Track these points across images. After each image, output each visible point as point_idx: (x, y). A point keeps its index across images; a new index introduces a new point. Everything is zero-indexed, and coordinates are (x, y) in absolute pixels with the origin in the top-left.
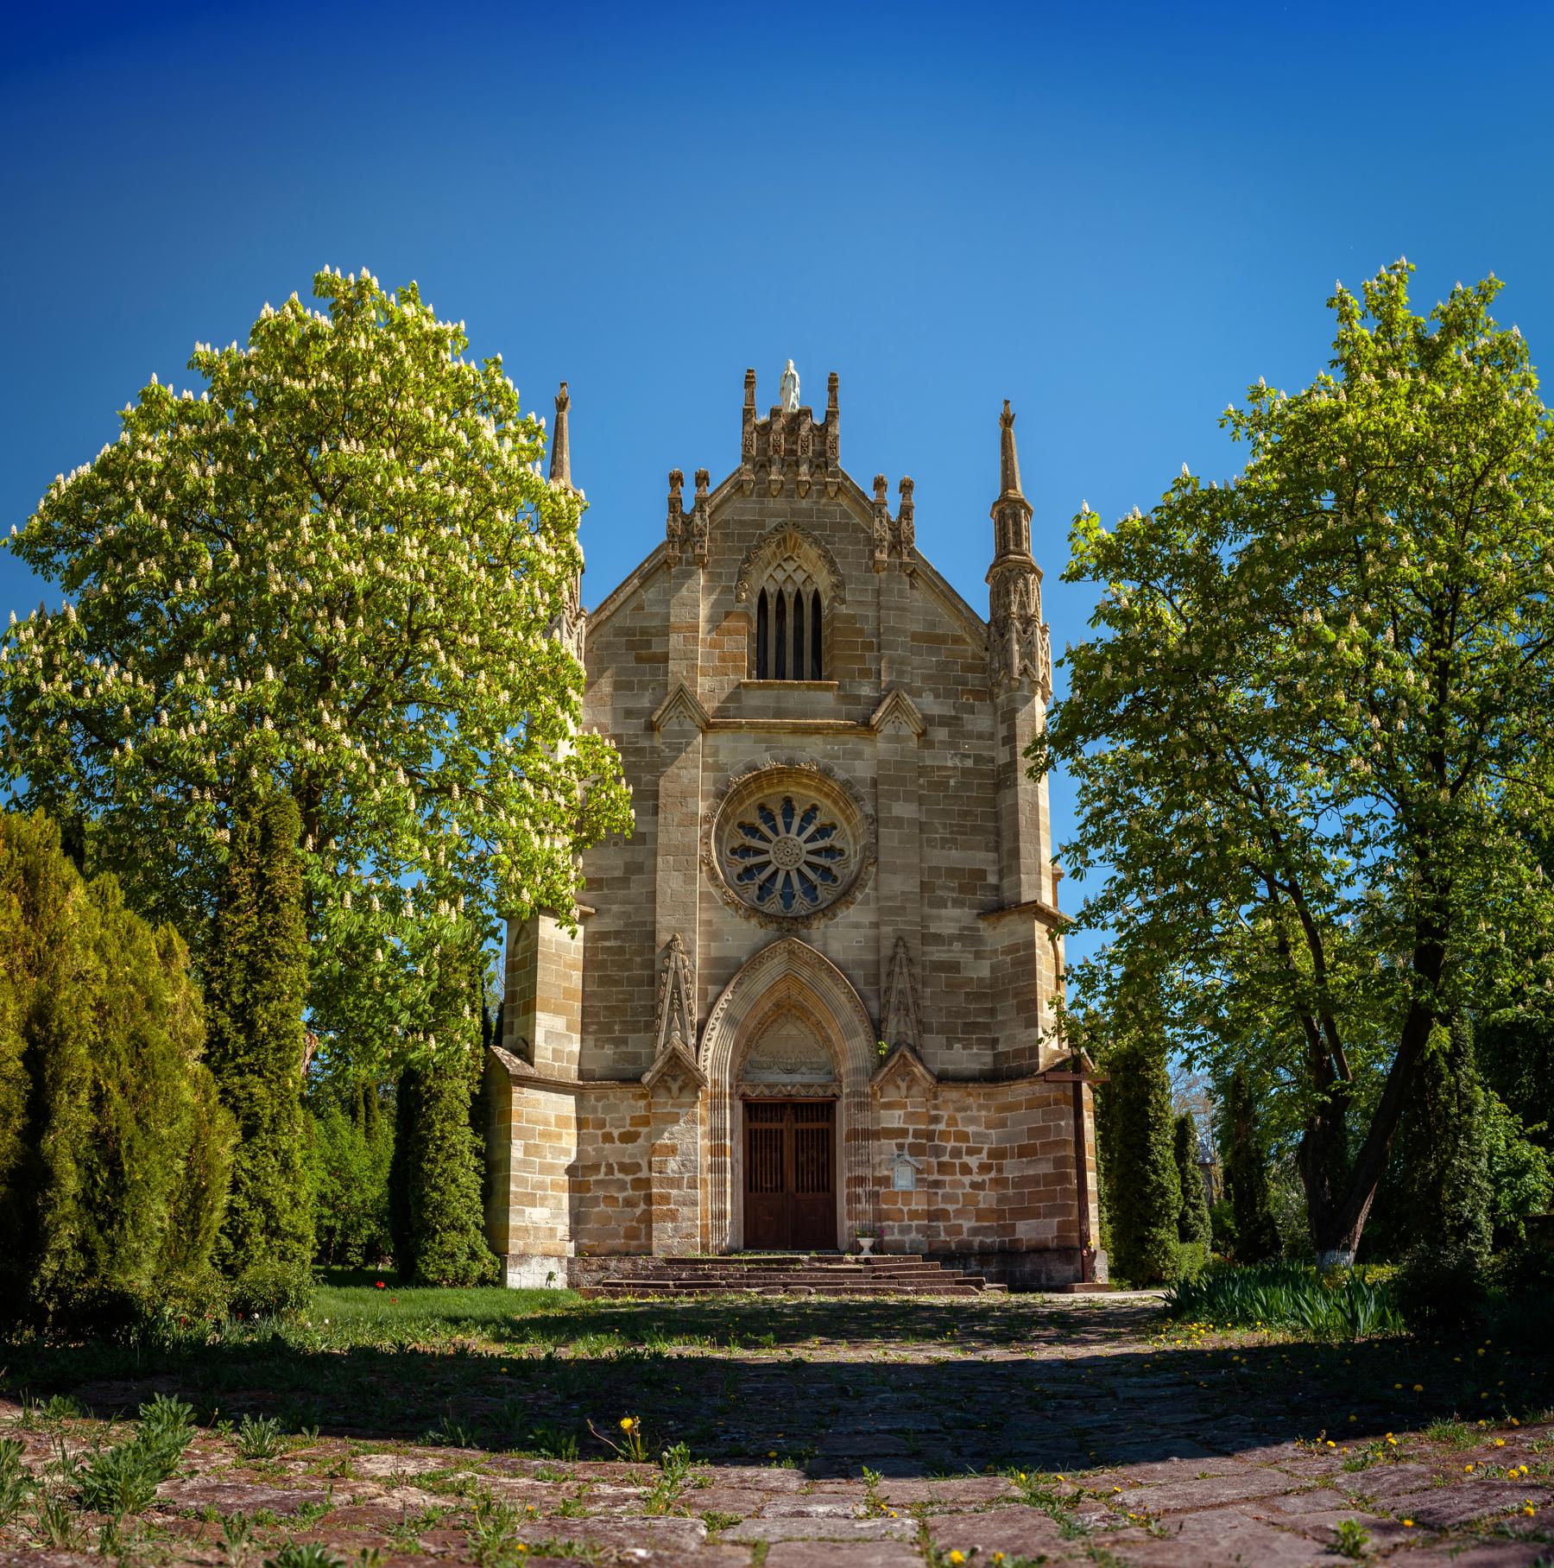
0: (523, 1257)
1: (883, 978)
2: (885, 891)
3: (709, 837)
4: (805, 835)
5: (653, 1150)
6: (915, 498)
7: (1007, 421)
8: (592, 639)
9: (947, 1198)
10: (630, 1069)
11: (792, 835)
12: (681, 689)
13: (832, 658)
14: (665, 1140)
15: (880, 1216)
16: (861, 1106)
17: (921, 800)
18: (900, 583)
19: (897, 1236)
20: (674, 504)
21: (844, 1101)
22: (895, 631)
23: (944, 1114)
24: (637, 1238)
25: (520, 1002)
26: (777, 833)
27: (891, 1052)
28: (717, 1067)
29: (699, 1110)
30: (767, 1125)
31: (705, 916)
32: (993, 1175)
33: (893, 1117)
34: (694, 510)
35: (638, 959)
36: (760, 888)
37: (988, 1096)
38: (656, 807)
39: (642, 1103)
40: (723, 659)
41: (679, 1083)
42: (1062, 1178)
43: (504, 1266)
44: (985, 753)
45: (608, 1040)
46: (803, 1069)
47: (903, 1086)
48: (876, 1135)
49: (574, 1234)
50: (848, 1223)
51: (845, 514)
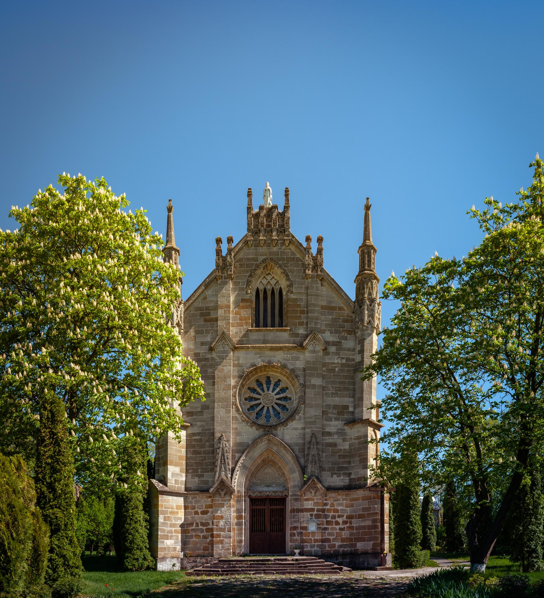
0: (164, 559)
1: (306, 450)
2: (308, 415)
3: (236, 394)
4: (275, 392)
5: (214, 518)
6: (324, 245)
7: (368, 208)
8: (186, 313)
9: (329, 534)
10: (205, 487)
11: (270, 392)
12: (224, 333)
13: (287, 317)
14: (219, 513)
15: (303, 541)
16: (296, 500)
17: (324, 377)
18: (317, 284)
19: (309, 549)
20: (218, 252)
21: (290, 498)
22: (314, 305)
23: (329, 502)
24: (208, 550)
25: (161, 462)
26: (264, 391)
27: (309, 479)
28: (239, 485)
29: (232, 502)
30: (259, 507)
31: (234, 426)
32: (348, 525)
33: (309, 504)
34: (227, 255)
35: (208, 444)
36: (257, 414)
37: (347, 495)
38: (214, 382)
39: (210, 500)
40: (241, 319)
41: (224, 492)
42: (375, 527)
43: (156, 562)
44: (351, 357)
45: (196, 476)
46: (274, 485)
47: (313, 492)
48: (302, 511)
49: (183, 549)
50: (290, 544)
51: (293, 253)
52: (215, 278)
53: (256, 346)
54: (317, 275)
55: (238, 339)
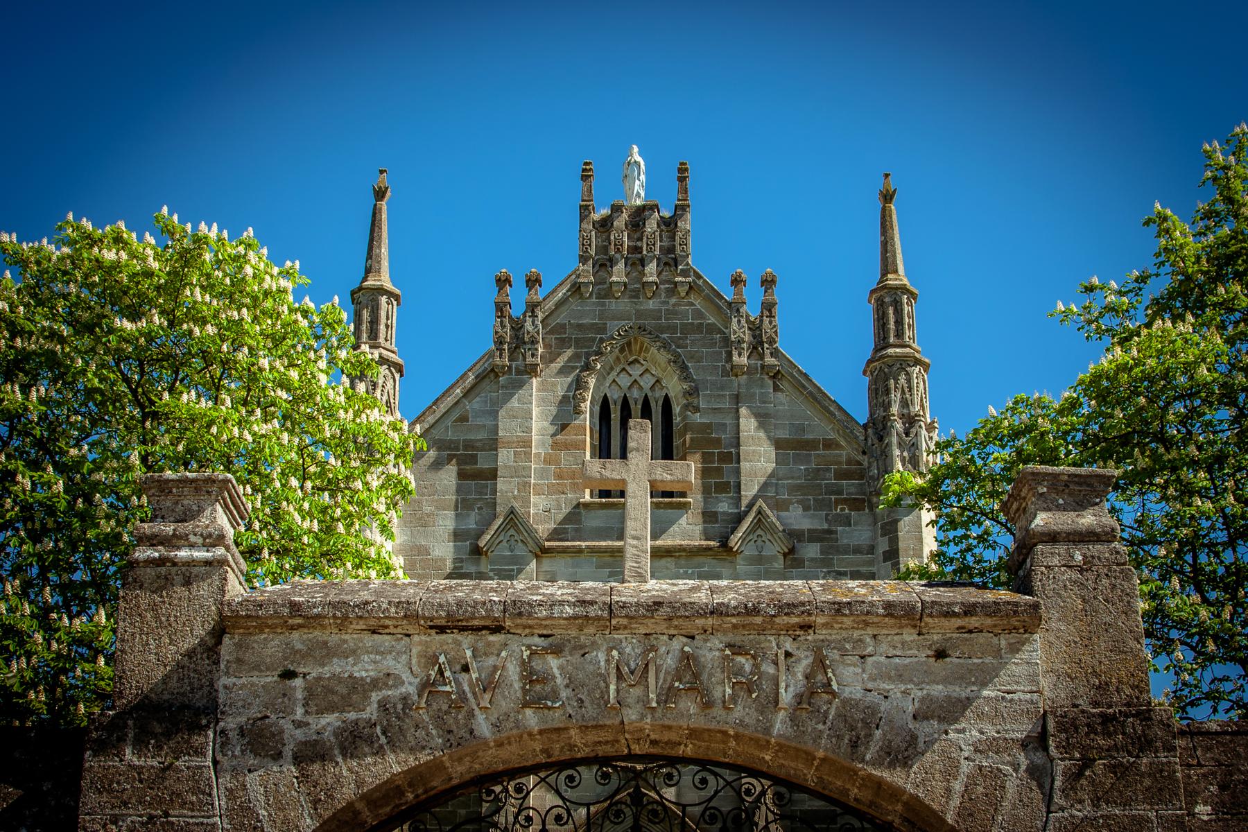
6: (777, 294)
12: (512, 511)
18: (762, 386)
40: (559, 476)
51: (698, 314)
52: (492, 370)
53: (600, 547)
54: (763, 367)
55: (553, 526)
